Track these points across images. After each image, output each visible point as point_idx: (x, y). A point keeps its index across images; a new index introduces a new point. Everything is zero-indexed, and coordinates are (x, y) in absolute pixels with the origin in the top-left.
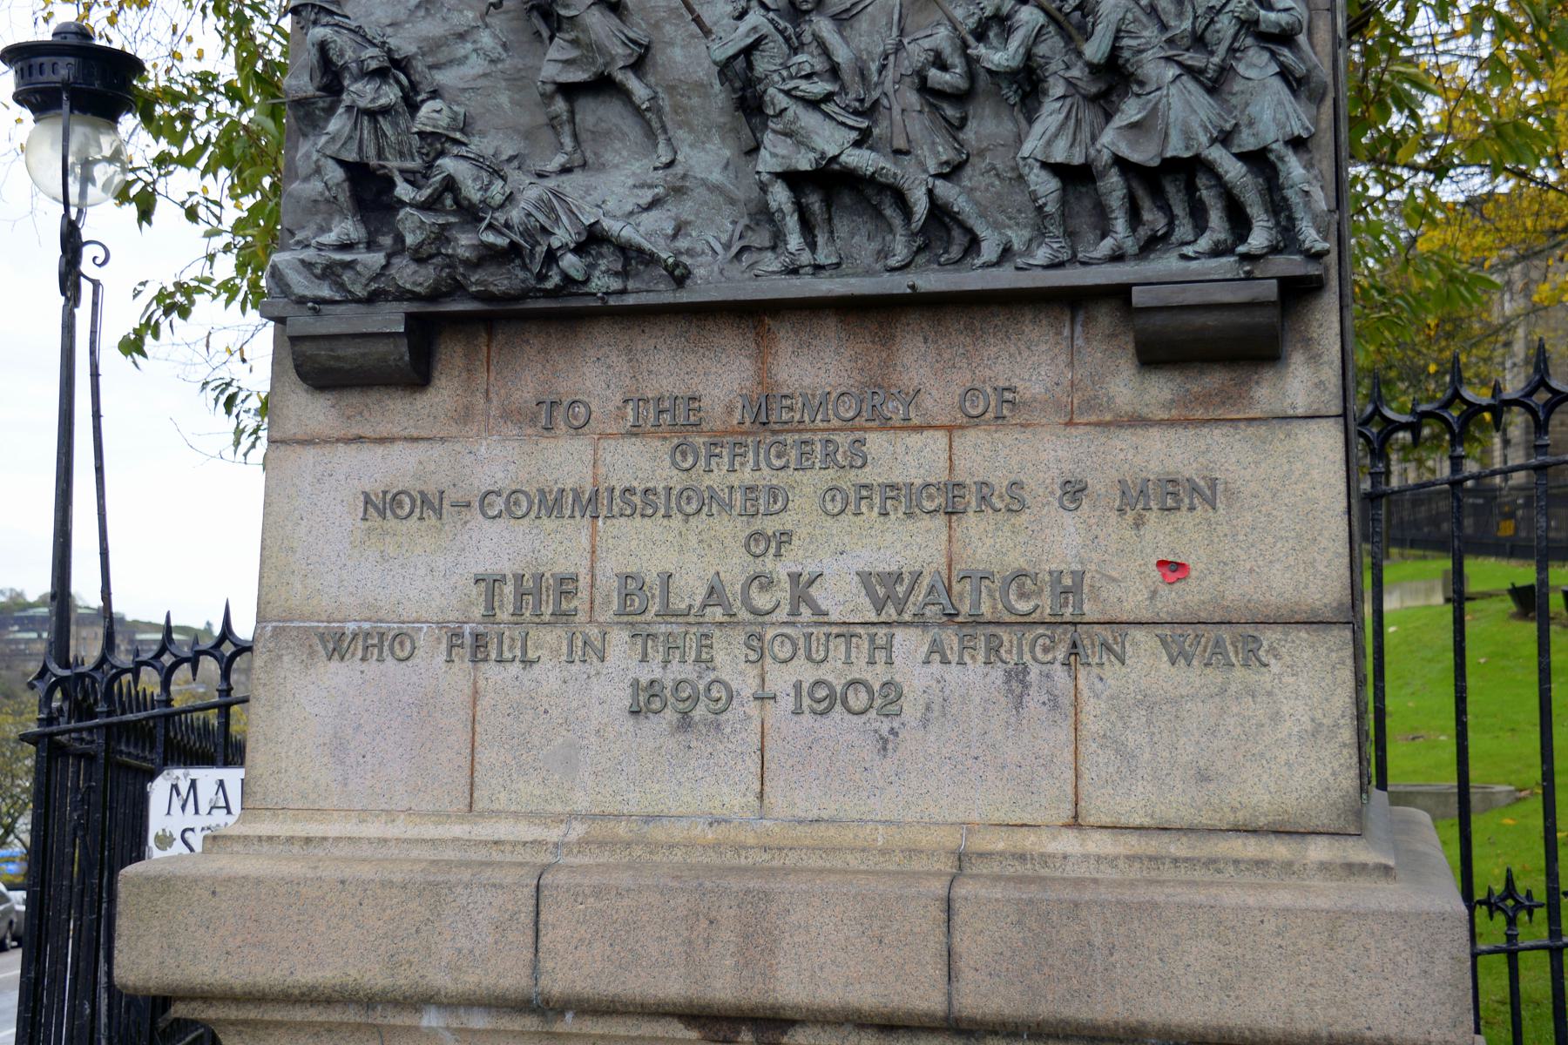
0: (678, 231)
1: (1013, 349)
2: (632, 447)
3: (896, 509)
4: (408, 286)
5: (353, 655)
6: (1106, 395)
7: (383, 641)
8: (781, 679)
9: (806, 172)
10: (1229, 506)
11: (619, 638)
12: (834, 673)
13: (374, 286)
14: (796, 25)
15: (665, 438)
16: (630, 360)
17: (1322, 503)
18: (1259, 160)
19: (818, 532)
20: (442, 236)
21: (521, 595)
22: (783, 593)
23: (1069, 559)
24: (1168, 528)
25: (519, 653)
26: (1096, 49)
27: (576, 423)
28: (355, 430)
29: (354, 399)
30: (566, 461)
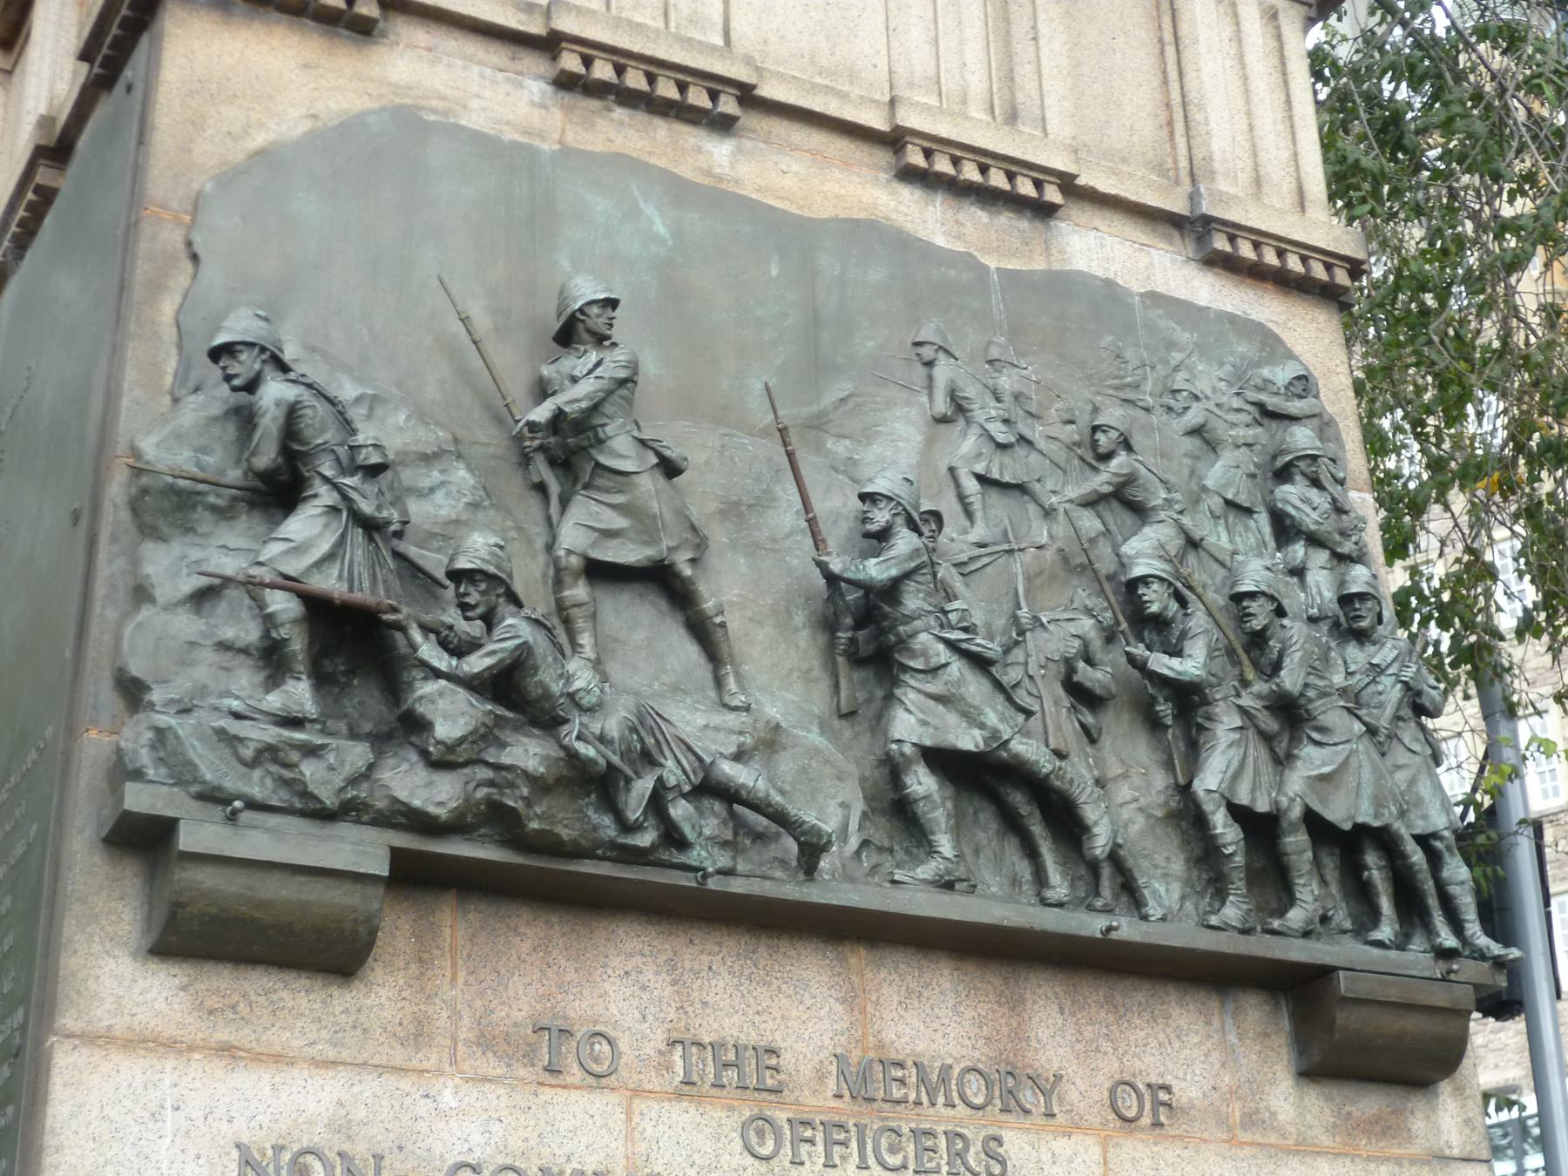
1: (1161, 1036)
2: (682, 1116)
4: (417, 803)
6: (1268, 1109)
15: (731, 1108)
20: (486, 736)
27: (598, 1069)
28: (223, 1035)
29: (221, 981)
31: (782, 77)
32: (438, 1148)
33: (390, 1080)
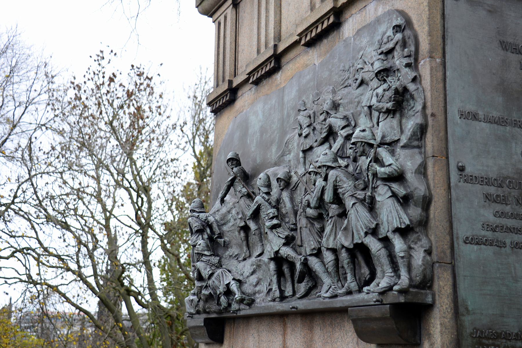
0: (258, 283)
18: (386, 241)
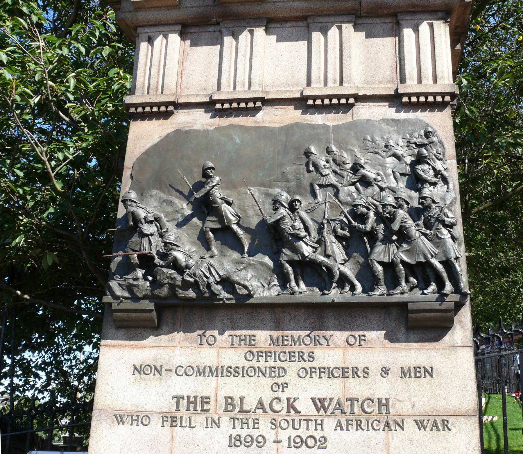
1: (365, 322)
3: (325, 376)
5: (128, 423)
7: (139, 418)
8: (284, 435)
9: (297, 260)
10: (438, 376)
11: (225, 421)
12: (303, 433)
13: (144, 293)
14: (293, 213)
16: (231, 322)
17: (467, 375)
19: (297, 383)
21: (189, 402)
22: (284, 404)
23: (385, 394)
24: (418, 384)
25: (188, 424)
26: (396, 226)
27: (211, 343)
30: (207, 356)
31: (274, 92)
32: (175, 363)
33: (165, 349)
